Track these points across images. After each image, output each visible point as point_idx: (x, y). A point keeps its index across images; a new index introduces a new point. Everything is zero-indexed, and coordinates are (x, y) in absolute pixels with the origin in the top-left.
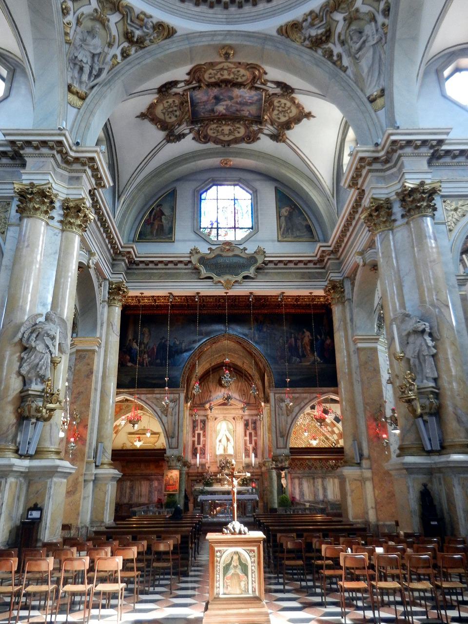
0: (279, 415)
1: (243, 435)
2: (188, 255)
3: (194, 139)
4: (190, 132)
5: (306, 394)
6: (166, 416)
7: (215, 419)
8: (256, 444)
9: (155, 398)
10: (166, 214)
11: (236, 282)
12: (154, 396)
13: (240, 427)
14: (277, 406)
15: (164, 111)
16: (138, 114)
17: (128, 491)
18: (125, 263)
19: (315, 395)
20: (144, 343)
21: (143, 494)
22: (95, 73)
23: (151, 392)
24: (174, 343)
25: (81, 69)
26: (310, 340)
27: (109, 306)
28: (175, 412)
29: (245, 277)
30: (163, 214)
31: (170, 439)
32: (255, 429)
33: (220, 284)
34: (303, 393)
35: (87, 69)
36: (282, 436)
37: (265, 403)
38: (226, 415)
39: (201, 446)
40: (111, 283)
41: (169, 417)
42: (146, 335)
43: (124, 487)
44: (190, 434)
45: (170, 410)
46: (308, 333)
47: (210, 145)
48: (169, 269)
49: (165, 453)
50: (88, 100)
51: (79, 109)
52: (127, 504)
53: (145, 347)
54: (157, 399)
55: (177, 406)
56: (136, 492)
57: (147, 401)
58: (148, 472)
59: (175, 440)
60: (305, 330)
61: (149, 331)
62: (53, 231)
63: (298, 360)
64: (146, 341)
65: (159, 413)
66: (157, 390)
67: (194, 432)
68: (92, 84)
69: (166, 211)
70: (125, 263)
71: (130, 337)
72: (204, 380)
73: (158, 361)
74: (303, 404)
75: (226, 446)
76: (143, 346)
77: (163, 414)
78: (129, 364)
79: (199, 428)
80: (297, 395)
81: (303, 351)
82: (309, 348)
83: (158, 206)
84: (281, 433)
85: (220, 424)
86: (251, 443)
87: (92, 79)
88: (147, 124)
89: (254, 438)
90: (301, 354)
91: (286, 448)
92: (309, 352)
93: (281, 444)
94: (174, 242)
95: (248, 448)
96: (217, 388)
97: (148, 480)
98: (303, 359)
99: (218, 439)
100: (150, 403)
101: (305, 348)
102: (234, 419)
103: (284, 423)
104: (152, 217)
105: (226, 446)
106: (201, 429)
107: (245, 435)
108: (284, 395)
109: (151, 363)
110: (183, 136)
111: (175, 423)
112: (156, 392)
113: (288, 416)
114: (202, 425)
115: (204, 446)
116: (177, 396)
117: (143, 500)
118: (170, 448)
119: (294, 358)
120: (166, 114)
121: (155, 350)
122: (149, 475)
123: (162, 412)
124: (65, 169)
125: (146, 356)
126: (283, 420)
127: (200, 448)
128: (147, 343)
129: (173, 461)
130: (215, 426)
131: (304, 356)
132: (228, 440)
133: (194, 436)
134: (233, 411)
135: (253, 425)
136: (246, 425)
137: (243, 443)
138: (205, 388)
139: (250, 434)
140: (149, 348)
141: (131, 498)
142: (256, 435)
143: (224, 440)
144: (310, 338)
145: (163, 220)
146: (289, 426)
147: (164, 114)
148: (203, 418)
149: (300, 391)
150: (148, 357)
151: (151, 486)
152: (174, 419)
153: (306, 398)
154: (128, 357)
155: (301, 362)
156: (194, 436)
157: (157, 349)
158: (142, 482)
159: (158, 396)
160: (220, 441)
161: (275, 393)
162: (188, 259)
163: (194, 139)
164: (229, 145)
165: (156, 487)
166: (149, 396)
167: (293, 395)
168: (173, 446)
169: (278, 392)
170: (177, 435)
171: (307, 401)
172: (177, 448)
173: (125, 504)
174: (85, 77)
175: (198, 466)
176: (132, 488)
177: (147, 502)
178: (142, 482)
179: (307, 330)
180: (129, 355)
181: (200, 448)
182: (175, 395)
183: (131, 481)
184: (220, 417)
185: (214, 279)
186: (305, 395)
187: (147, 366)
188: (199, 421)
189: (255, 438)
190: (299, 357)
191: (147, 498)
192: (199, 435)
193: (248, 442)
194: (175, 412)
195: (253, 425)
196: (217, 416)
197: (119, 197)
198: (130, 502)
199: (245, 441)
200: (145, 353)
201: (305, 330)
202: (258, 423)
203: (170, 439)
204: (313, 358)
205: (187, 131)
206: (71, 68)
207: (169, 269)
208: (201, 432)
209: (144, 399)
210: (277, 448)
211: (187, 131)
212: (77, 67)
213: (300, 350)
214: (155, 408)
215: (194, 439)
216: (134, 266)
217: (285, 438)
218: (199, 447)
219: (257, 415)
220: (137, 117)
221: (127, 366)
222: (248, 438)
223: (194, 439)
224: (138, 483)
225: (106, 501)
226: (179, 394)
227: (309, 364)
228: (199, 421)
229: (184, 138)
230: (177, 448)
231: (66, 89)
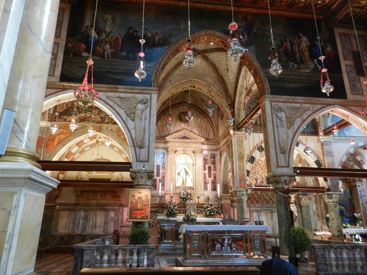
0: (277, 126)
1: (203, 168)
5: (309, 105)
6: (133, 120)
7: (175, 152)
8: (215, 177)
9: (119, 97)
12: (118, 94)
13: (200, 162)
14: (275, 116)
17: (81, 221)
19: (319, 107)
20: (105, 32)
21: (97, 225)
23: (114, 90)
26: (308, 45)
28: (146, 116)
31: (138, 150)
32: (214, 163)
34: (305, 103)
36: (283, 152)
37: (234, 130)
38: (186, 149)
39: (160, 177)
41: (137, 121)
42: (109, 23)
43: (78, 217)
45: (138, 112)
46: (305, 39)
49: (131, 167)
52: (80, 235)
53: (107, 36)
54: (121, 98)
55: (148, 109)
56: (91, 223)
58: (104, 202)
59: (144, 151)
60: (301, 35)
61: (113, 19)
63: (296, 65)
64: (108, 29)
65: (124, 116)
66: (121, 88)
71: (88, 23)
72: (164, 114)
73: (124, 54)
74: (305, 116)
75: (184, 179)
76: (104, 35)
77: (128, 118)
80: (298, 105)
81: (301, 57)
82: (307, 54)
84: (281, 149)
85: (178, 158)
86: (210, 176)
89: (213, 172)
90: (299, 60)
91: (288, 167)
92: (308, 59)
93: (282, 163)
95: (206, 181)
96: (177, 123)
97: (105, 210)
98: (301, 66)
99: (177, 172)
100: (111, 103)
101: (303, 53)
102: (194, 152)
103: (285, 137)
105: (184, 179)
107: (205, 169)
108: (282, 104)
109: (114, 55)
111: (144, 131)
112: (119, 90)
113: (288, 128)
115: (163, 177)
116: (148, 96)
117: (99, 231)
118: (138, 161)
119: (291, 64)
121: (120, 40)
122: (105, 206)
123: (128, 115)
125: (108, 46)
126: (284, 133)
127: (160, 179)
128: (110, 32)
129: (142, 177)
130: (175, 159)
131: (302, 62)
132: (187, 173)
134: (193, 145)
135: (212, 159)
136: (205, 160)
137: (203, 177)
138: (165, 122)
139: (210, 168)
140: (112, 37)
141: (84, 229)
142: (215, 170)
143: (183, 173)
144: (308, 43)
146: (290, 140)
149: (300, 101)
150: (111, 48)
151: (107, 216)
152: (143, 125)
153: (309, 110)
154: (84, 46)
155: (299, 69)
157: (122, 40)
158: (98, 213)
159: (123, 95)
160: (179, 174)
161: (271, 102)
165: (112, 218)
167: (293, 105)
168: (142, 159)
169: (275, 100)
170: (147, 144)
171: (310, 112)
173: (78, 235)
176: (86, 218)
177: (102, 233)
178: (98, 213)
179: (304, 35)
180: (85, 44)
181: (160, 179)
182: (145, 95)
183: (86, 211)
184: (180, 150)
186: (307, 106)
189: (215, 172)
190: (296, 62)
191: (102, 229)
193: (207, 176)
194: (146, 116)
195: (212, 159)
196: (177, 149)
198: (84, 233)
199: (204, 174)
200: (106, 42)
201: (301, 35)
202: (218, 157)
203: (138, 150)
204: (314, 65)
209: (104, 98)
210: (278, 166)
213: (298, 55)
214: (118, 109)
217: (287, 155)
218: (158, 178)
219: (216, 150)
221: (82, 57)
222: (207, 172)
224: (93, 213)
225: (9, 230)
226: (151, 94)
227: (308, 71)
230: (148, 161)
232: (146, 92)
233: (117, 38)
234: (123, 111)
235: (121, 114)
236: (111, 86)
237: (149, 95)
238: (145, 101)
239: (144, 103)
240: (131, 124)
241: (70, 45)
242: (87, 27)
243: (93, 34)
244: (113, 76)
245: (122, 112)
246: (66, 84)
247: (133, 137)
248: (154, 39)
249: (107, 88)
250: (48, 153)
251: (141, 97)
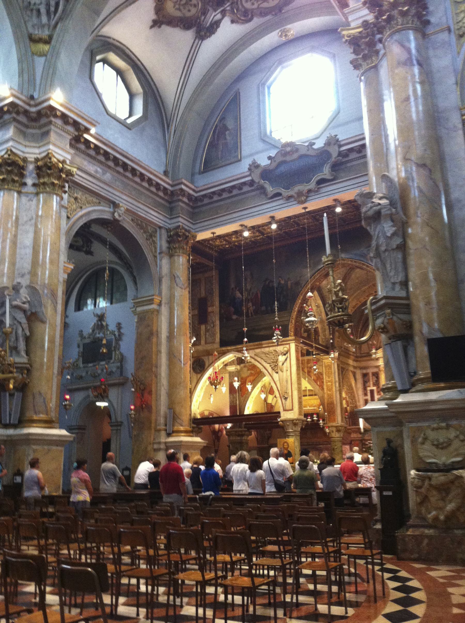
2: (248, 173)
3: (233, 22)
4: (223, 16)
6: (277, 373)
10: (230, 127)
11: (309, 191)
12: (263, 350)
15: (177, 6)
16: (151, 23)
18: (184, 202)
22: (52, 9)
24: (279, 283)
25: (39, 11)
27: (171, 256)
29: (322, 182)
30: (226, 129)
33: (293, 200)
35: (43, 10)
40: (168, 230)
44: (360, 392)
47: (257, 21)
48: (236, 196)
50: (53, 42)
51: (46, 56)
57: (256, 358)
62: (27, 196)
64: (249, 287)
65: (270, 369)
67: (365, 389)
68: (53, 23)
69: (230, 124)
70: (184, 202)
71: (233, 286)
73: (263, 308)
78: (234, 317)
79: (371, 383)
83: (220, 121)
87: (52, 16)
88: (167, 30)
94: (240, 160)
97: (317, 449)
100: (259, 359)
104: (216, 136)
106: (374, 385)
109: (256, 312)
110: (215, 25)
112: (264, 346)
114: (375, 379)
118: (285, 410)
120: (182, 8)
121: (259, 295)
122: (317, 445)
124: (34, 128)
125: (250, 304)
133: (366, 394)
145: (228, 137)
147: (179, 9)
148: (375, 370)
150: (253, 305)
154: (232, 309)
156: (366, 394)
157: (261, 295)
162: (249, 178)
163: (233, 22)
164: (280, 11)
166: (258, 351)
168: (287, 408)
170: (290, 394)
172: (292, 410)
174: (44, 19)
175: (362, 430)
185: (283, 194)
187: (252, 316)
188: (371, 375)
192: (372, 392)
197: (168, 126)
203: (284, 401)
205: (219, 16)
206: (28, 16)
207: (236, 196)
208: (375, 388)
211: (219, 16)
212: (35, 12)
215: (366, 398)
216: (200, 204)
220: (152, 27)
223: (366, 398)
226: (289, 344)
228: (371, 375)
229: (218, 26)
230: (292, 410)
231: (27, 41)
232: (285, 343)
233: (257, 294)
234: (269, 365)
235: (267, 368)
236: (256, 343)
237: (288, 346)
238: (285, 353)
239: (285, 355)
240: (276, 376)
241: (223, 311)
242: (233, 289)
243: (238, 295)
244: (257, 333)
245: (267, 366)
246: (224, 349)
247: (279, 389)
248: (287, 285)
249: (254, 345)
250: (242, 396)
251: (280, 349)
